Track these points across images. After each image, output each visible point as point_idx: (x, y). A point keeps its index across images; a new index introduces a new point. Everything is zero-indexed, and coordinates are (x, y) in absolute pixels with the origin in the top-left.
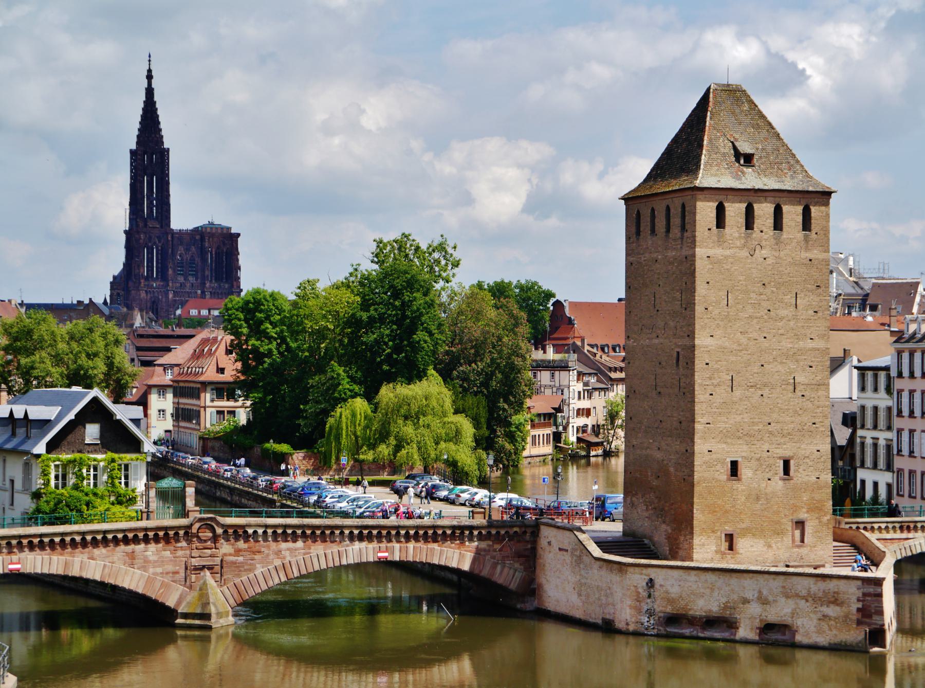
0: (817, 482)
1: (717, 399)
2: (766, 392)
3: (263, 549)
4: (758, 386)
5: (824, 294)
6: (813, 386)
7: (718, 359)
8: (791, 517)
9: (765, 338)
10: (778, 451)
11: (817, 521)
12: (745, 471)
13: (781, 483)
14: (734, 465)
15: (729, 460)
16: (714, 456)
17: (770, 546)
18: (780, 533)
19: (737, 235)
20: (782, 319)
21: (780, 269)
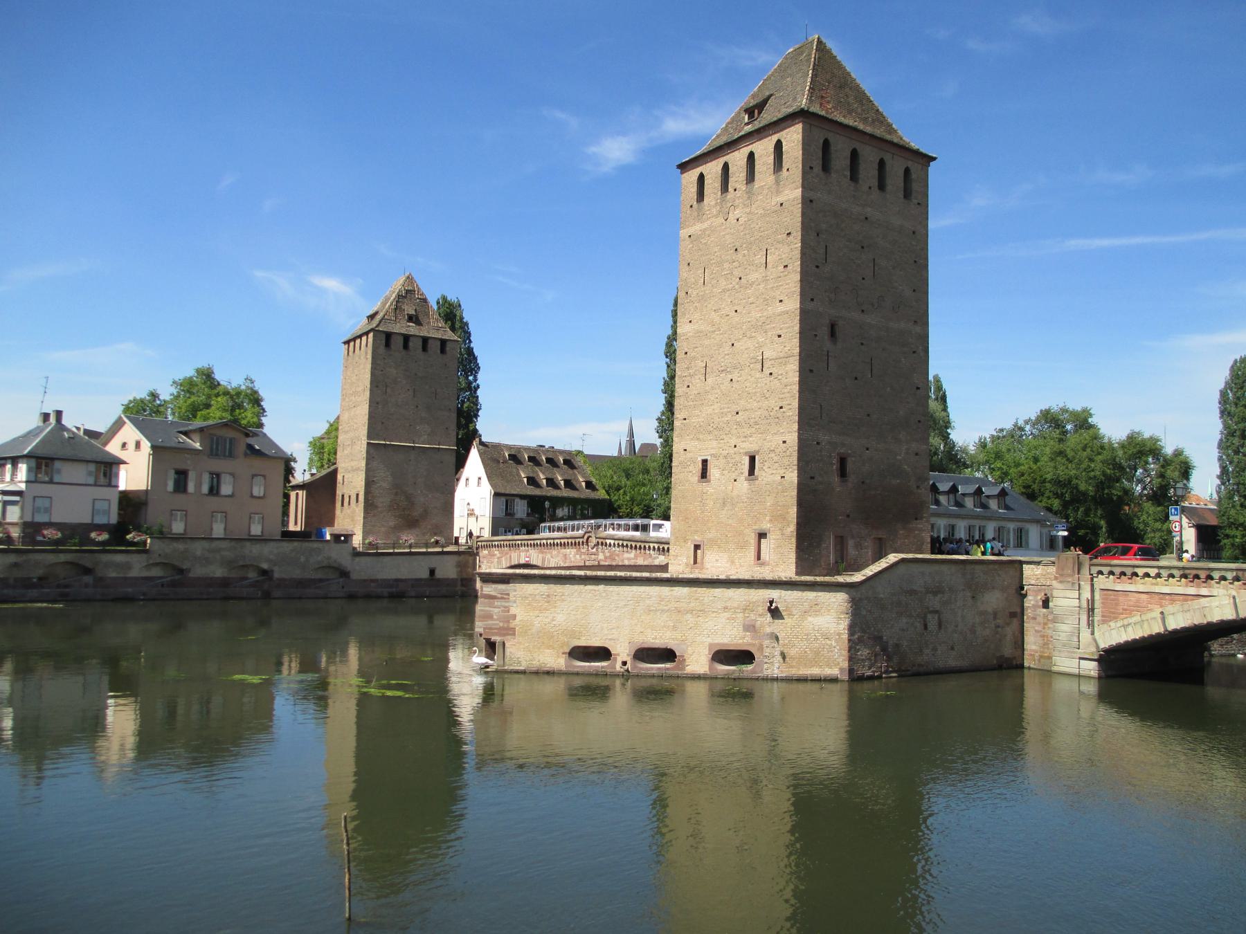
0: (780, 484)
1: (693, 391)
2: (735, 376)
3: (616, 558)
4: (728, 370)
5: (796, 241)
6: (780, 361)
7: (694, 346)
8: (754, 527)
9: (736, 311)
10: (744, 445)
11: (778, 532)
12: (713, 472)
13: (746, 484)
14: (705, 462)
15: (700, 459)
16: (689, 455)
17: (733, 562)
18: (742, 546)
19: (713, 203)
20: (753, 283)
21: (752, 226)
